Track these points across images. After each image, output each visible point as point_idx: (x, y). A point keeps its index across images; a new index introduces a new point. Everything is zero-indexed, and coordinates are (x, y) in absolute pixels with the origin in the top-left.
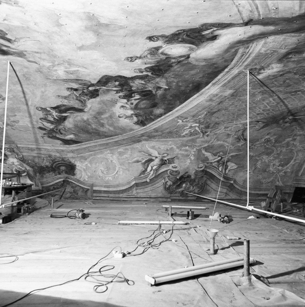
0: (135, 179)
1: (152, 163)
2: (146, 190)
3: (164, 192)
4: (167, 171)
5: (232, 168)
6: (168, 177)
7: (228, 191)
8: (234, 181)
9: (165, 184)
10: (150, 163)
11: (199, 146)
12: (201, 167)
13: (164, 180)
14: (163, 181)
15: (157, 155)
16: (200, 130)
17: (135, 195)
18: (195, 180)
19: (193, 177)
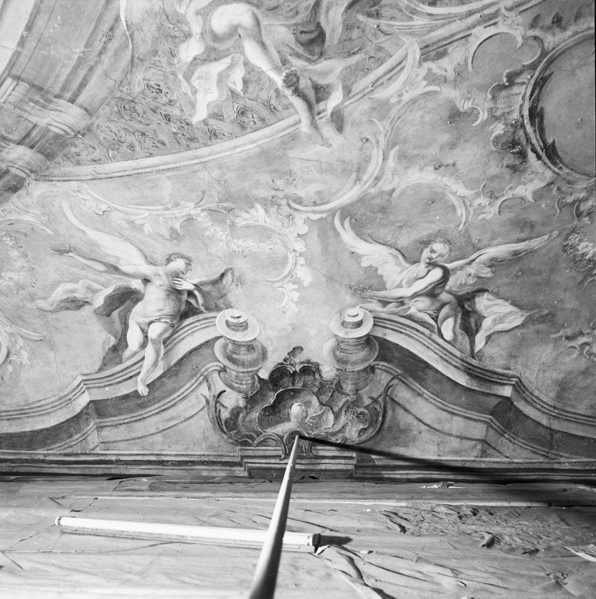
0: (88, 382)
1: (138, 308)
2: (140, 429)
3: (214, 437)
4: (209, 344)
5: (499, 327)
7: (491, 432)
8: (514, 386)
9: (212, 403)
10: (129, 310)
11: (315, 204)
12: (359, 324)
13: (205, 386)
14: (204, 390)
16: (277, 69)
17: (98, 451)
18: (339, 383)
19: (328, 371)
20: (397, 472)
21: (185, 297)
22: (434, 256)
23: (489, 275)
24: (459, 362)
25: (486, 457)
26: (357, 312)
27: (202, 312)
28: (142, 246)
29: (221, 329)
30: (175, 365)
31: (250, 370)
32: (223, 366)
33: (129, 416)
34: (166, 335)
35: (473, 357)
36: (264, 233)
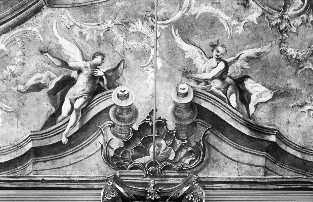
0: (33, 136)
1: (72, 90)
2: (58, 163)
3: (104, 166)
4: (107, 110)
6: (111, 127)
7: (268, 162)
8: (276, 135)
9: (104, 147)
10: (66, 91)
12: (186, 95)
15: (81, 64)
17: (31, 175)
19: (171, 125)
20: (214, 185)
21: (98, 81)
22: (219, 54)
23: (248, 67)
24: (243, 121)
25: (268, 176)
26: (184, 87)
27: (105, 90)
28: (82, 49)
29: (114, 100)
30: (86, 124)
31: (128, 124)
32: (113, 123)
33: (54, 156)
34: (84, 106)
35: (250, 118)
36: (140, 36)
